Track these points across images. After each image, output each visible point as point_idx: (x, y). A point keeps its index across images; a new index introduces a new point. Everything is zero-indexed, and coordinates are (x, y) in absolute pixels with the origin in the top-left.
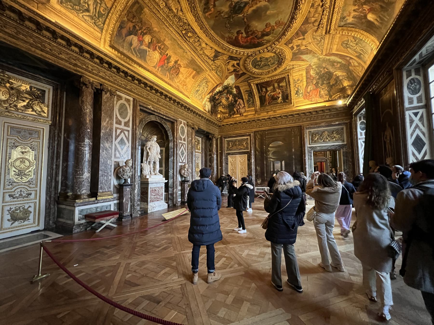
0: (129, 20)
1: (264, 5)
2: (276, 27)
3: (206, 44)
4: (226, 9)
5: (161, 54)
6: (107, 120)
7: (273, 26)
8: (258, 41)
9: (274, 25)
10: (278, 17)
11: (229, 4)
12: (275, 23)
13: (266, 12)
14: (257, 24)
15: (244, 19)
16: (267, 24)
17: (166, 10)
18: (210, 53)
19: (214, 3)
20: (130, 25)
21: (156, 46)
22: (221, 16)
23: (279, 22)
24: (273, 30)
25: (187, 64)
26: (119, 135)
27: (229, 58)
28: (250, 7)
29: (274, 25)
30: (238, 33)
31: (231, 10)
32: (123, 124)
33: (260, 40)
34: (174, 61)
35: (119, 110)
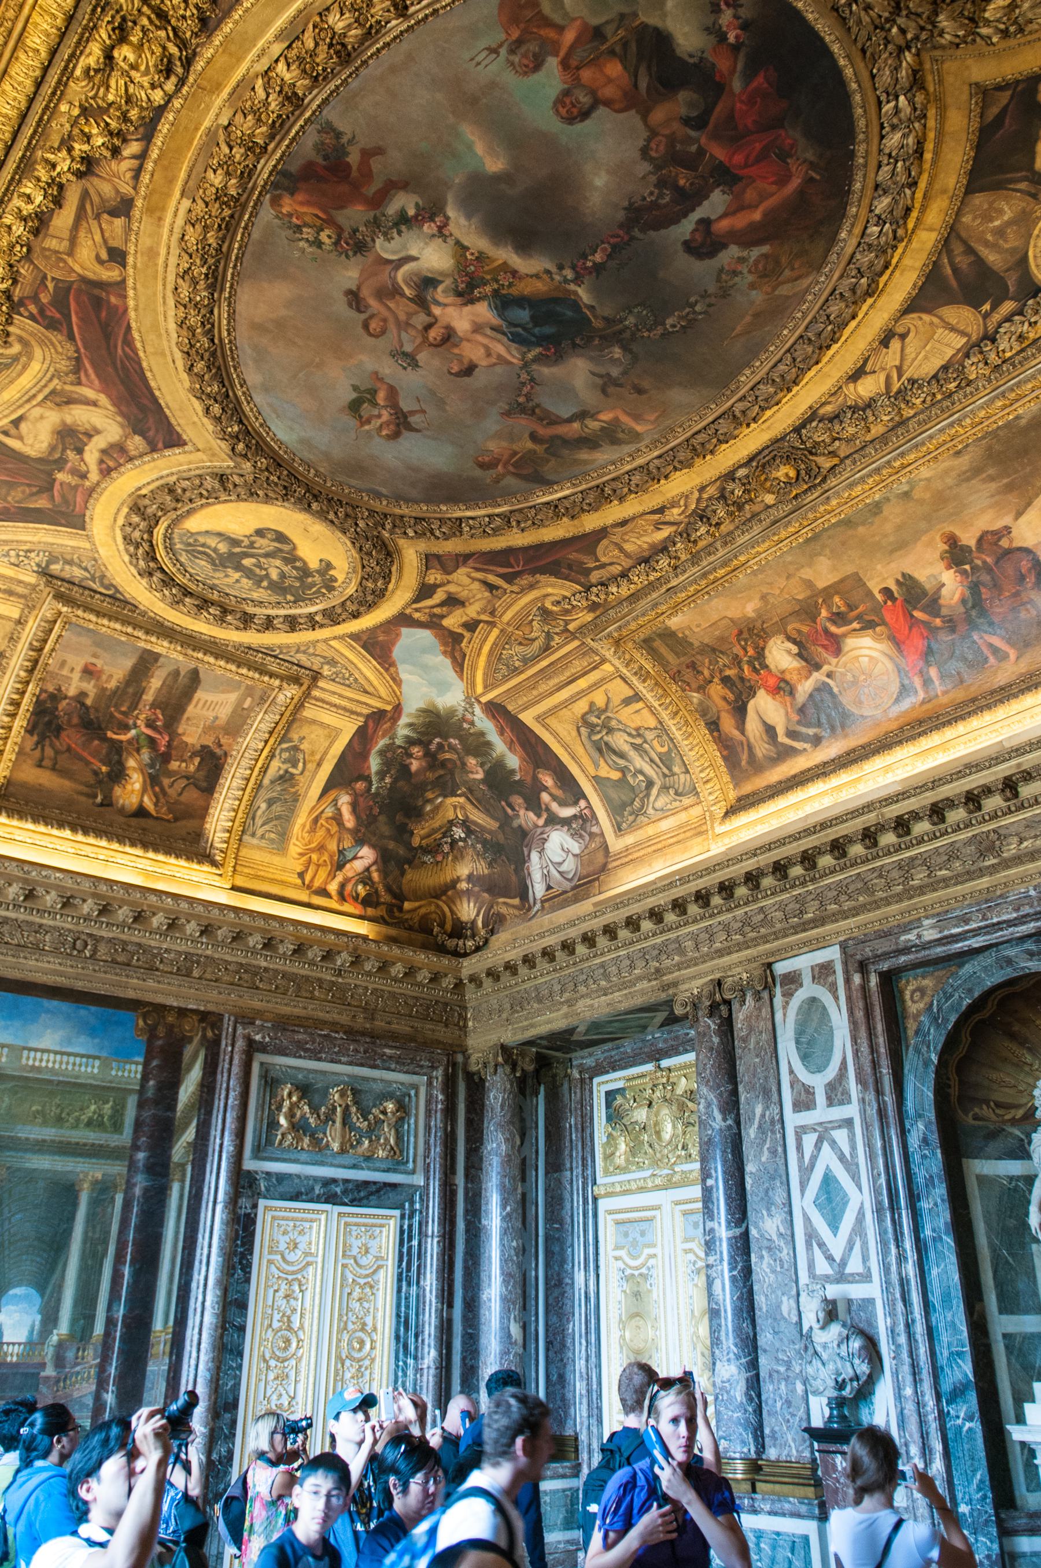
0: (701, 689)
1: (469, 217)
2: (569, 36)
3: (857, 375)
4: (578, 372)
5: (868, 625)
6: (759, 1110)
7: (565, 64)
8: (737, 85)
9: (552, 63)
10: (493, 85)
11: (546, 371)
12: (537, 67)
13: (497, 178)
14: (600, 181)
15: (598, 268)
16: (570, 120)
17: (664, 562)
18: (935, 343)
19: (570, 420)
20: (717, 690)
21: (826, 631)
22: (624, 373)
23: (519, 42)
24: (598, 33)
25: (1010, 488)
26: (814, 1158)
27: (999, 186)
28: (514, 273)
29: (552, 63)
30: (706, 244)
31: (575, 346)
32: (820, 1098)
33: (723, 64)
34: (941, 565)
35: (797, 1042)
